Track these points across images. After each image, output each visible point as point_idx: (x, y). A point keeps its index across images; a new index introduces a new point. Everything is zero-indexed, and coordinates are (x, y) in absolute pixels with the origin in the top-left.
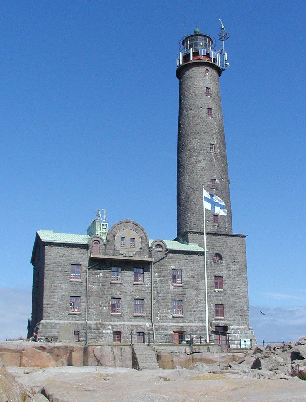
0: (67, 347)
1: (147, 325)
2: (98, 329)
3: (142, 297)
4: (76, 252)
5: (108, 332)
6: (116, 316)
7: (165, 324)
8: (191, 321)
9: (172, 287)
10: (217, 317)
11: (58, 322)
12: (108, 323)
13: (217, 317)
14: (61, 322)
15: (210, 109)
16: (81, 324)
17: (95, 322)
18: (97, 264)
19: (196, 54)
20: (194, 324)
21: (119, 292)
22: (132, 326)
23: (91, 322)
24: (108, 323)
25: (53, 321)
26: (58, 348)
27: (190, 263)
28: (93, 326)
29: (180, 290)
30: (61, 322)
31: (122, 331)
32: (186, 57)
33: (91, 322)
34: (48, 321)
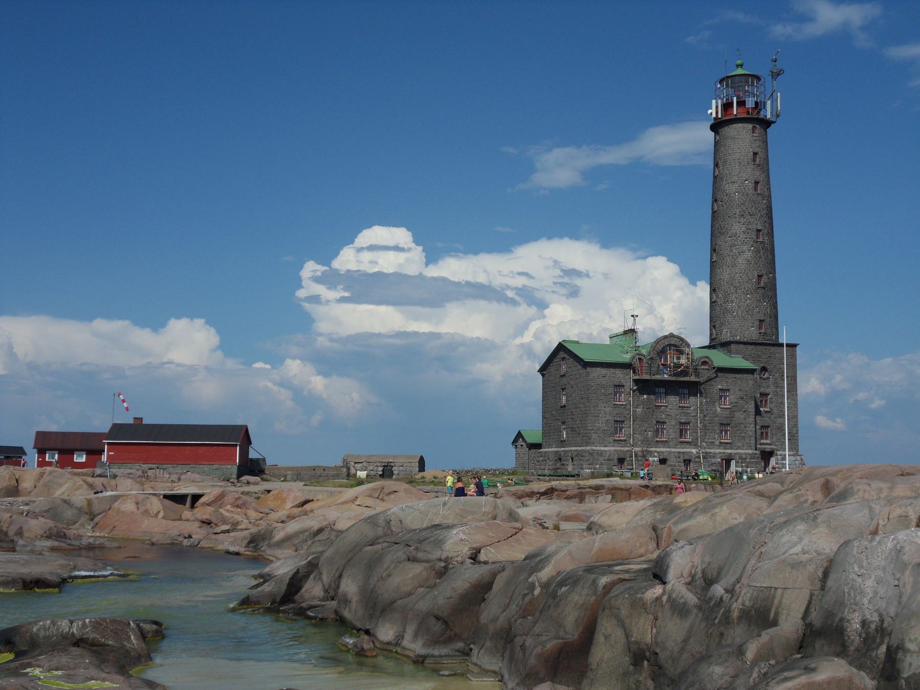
0: (667, 486)
1: (694, 451)
2: (644, 456)
3: (688, 421)
4: (619, 372)
5: (654, 459)
6: (661, 442)
7: (712, 451)
8: (739, 448)
9: (719, 410)
10: (762, 441)
11: (603, 448)
12: (653, 449)
13: (762, 441)
14: (606, 449)
15: (757, 183)
16: (628, 451)
17: (640, 449)
18: (645, 387)
19: (741, 103)
20: (742, 451)
21: (663, 416)
22: (679, 453)
23: (637, 449)
24: (653, 449)
25: (598, 448)
26: (660, 486)
27: (739, 382)
28: (640, 454)
29: (727, 412)
30: (606, 449)
31: (668, 458)
32: (727, 106)
33: (637, 449)
34: (594, 448)
